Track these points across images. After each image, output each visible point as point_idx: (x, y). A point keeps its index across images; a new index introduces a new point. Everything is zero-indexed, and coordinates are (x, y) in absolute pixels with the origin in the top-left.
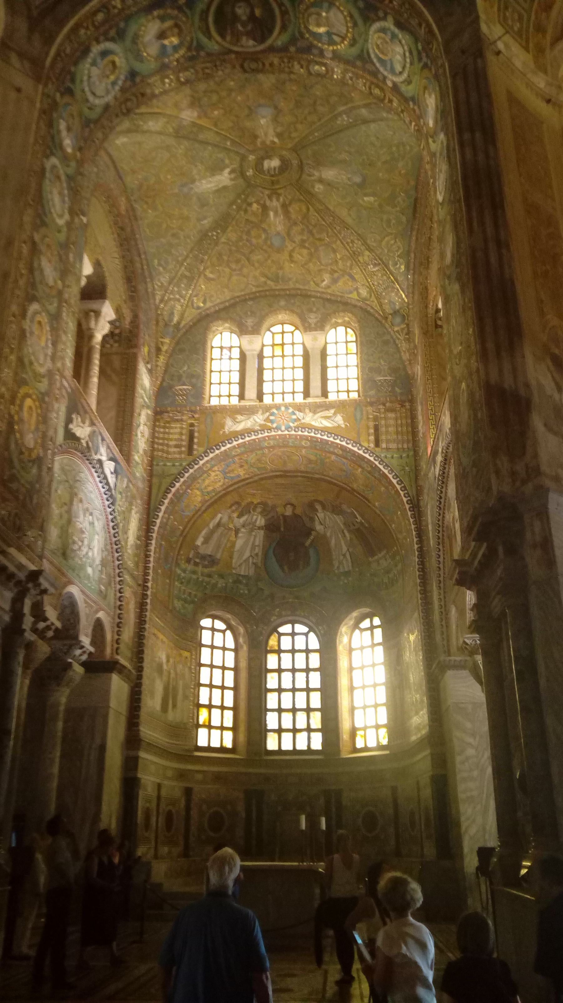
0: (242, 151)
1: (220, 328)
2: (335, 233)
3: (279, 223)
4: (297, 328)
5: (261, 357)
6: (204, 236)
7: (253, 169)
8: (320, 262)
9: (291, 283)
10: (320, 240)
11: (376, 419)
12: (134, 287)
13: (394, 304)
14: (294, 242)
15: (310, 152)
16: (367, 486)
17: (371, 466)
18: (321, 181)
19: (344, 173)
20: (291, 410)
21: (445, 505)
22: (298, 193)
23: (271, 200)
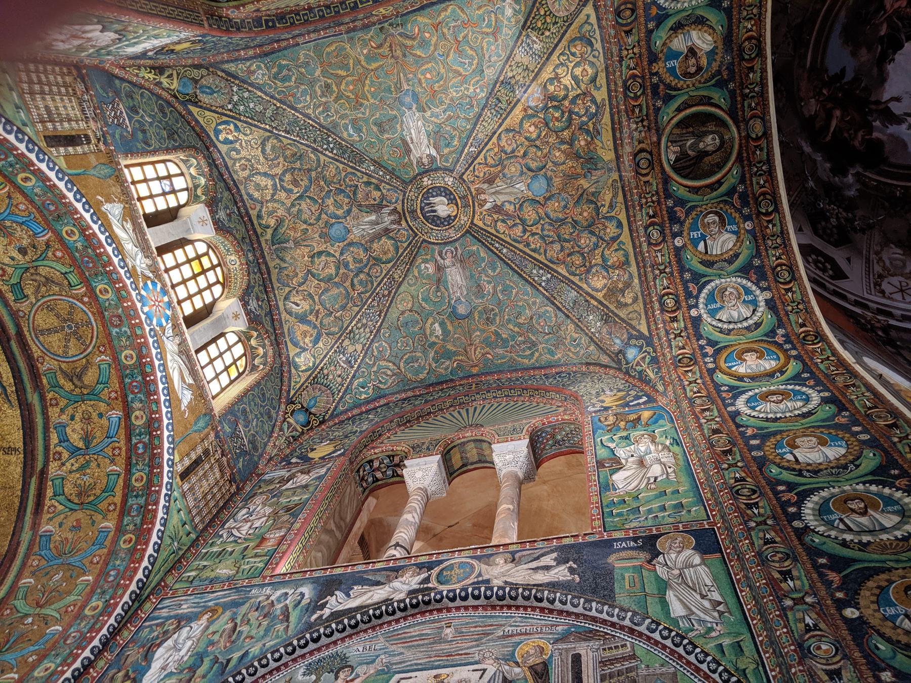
0: (459, 168)
1: (193, 171)
2: (367, 300)
3: (363, 229)
4: (223, 285)
5: (182, 243)
6: (329, 131)
9: (278, 261)
10: (353, 285)
11: (206, 452)
13: (314, 406)
14: (342, 254)
15: (475, 248)
16: (79, 495)
17: (150, 483)
18: (439, 269)
19: (465, 293)
20: (169, 313)
21: (303, 656)
22: (405, 245)
23: (390, 214)
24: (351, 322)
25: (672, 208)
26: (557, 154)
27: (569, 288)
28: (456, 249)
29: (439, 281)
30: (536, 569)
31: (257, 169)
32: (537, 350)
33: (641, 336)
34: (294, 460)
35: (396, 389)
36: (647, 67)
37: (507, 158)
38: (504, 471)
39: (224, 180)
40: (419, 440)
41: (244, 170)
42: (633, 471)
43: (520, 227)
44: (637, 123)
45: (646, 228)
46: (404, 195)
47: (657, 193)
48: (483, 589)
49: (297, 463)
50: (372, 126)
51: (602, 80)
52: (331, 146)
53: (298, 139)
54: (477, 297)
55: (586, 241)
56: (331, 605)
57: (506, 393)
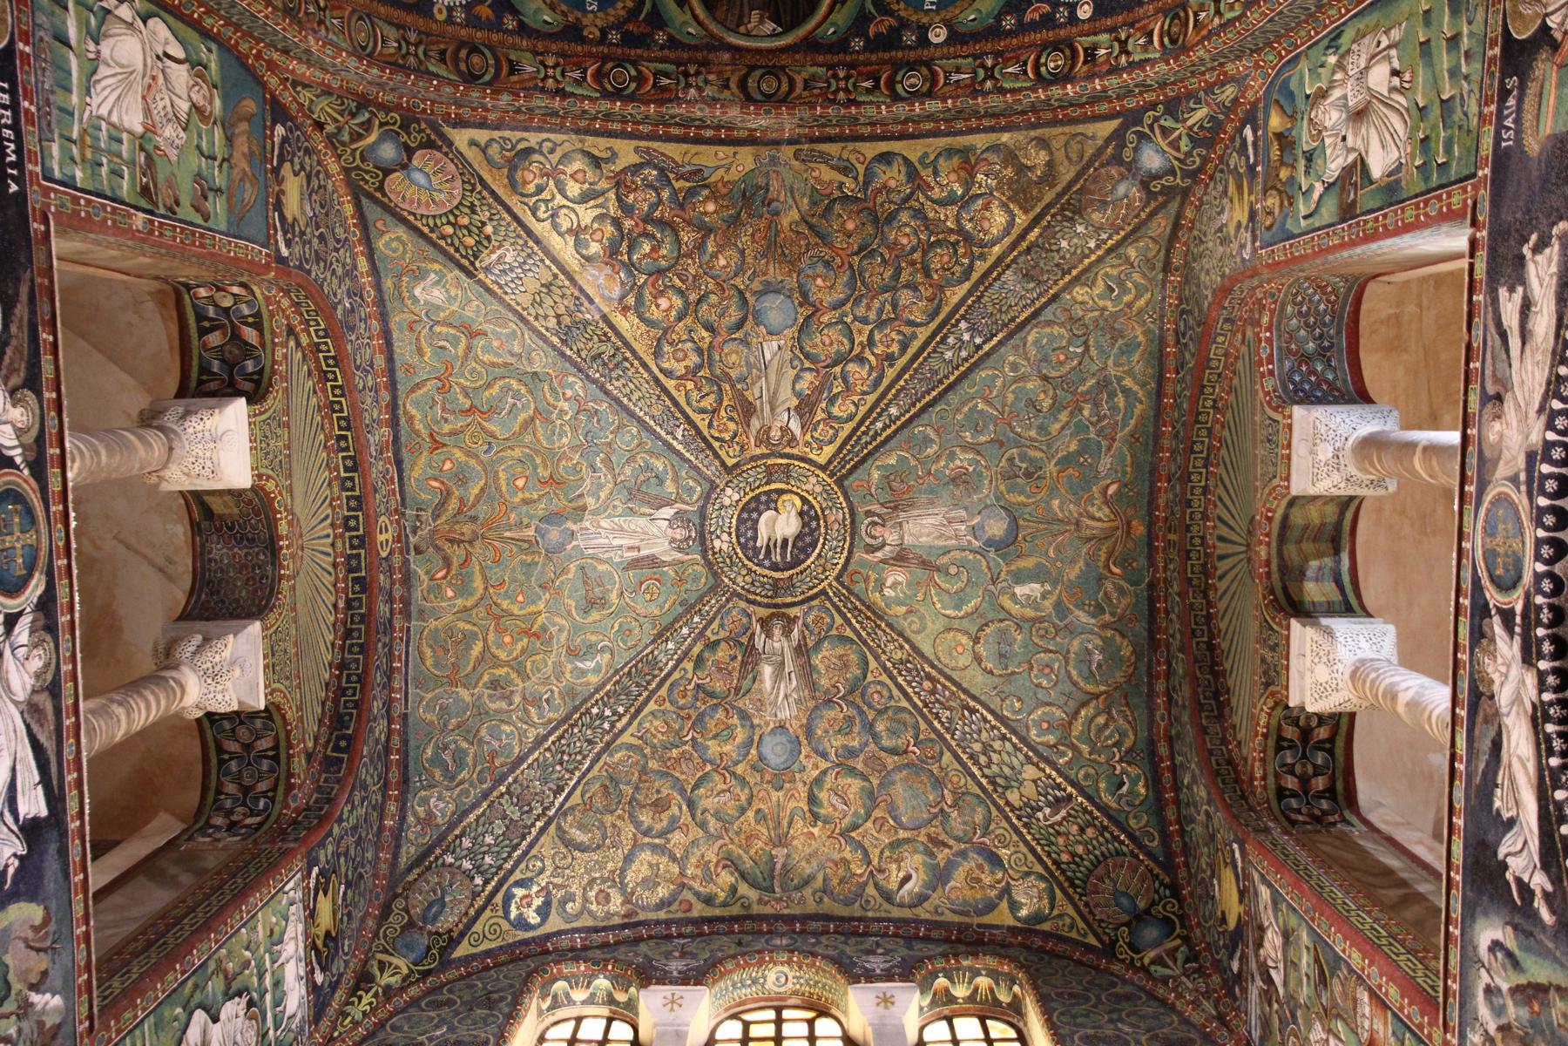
1: (579, 995)
2: (934, 730)
3: (786, 696)
4: (824, 1013)
6: (577, 711)
7: (730, 534)
8: (894, 819)
9: (808, 892)
10: (893, 751)
12: (349, 738)
13: (1132, 900)
14: (824, 756)
15: (876, 475)
19: (963, 513)
22: (839, 620)
23: (769, 635)
24: (973, 776)
25: (868, 40)
26: (722, 262)
27: (997, 284)
28: (869, 514)
29: (926, 564)
30: (1525, 335)
31: (613, 872)
32: (1119, 379)
33: (1118, 137)
34: (1235, 966)
35: (1141, 714)
36: (587, 48)
37: (710, 366)
38: (1352, 470)
39: (618, 943)
40: (1254, 673)
41: (608, 898)
42: (1373, 131)
43: (851, 367)
44: (688, 86)
45: (896, 98)
46: (739, 596)
47: (831, 67)
48: (1546, 469)
49: (1243, 958)
50: (590, 619)
51: (599, 145)
52: (608, 712)
53: (577, 774)
54: (977, 489)
55: (904, 234)
56: (1525, 869)
57: (1200, 463)
